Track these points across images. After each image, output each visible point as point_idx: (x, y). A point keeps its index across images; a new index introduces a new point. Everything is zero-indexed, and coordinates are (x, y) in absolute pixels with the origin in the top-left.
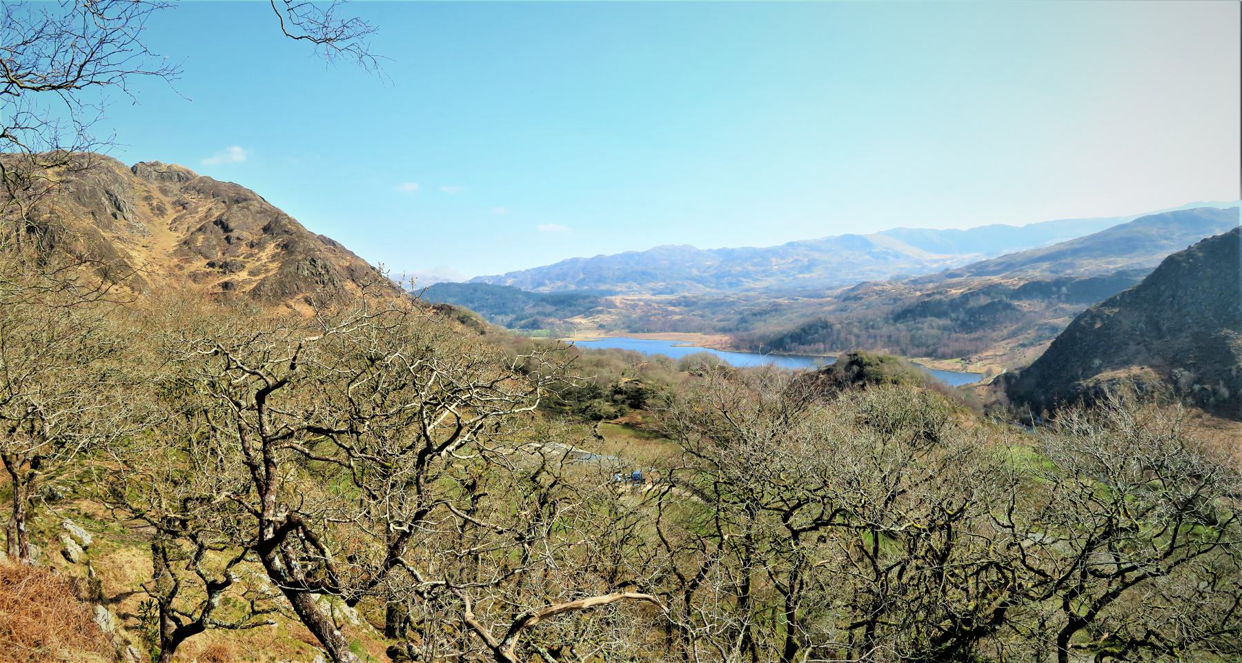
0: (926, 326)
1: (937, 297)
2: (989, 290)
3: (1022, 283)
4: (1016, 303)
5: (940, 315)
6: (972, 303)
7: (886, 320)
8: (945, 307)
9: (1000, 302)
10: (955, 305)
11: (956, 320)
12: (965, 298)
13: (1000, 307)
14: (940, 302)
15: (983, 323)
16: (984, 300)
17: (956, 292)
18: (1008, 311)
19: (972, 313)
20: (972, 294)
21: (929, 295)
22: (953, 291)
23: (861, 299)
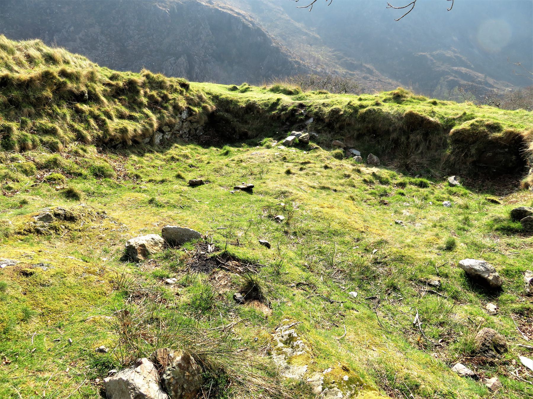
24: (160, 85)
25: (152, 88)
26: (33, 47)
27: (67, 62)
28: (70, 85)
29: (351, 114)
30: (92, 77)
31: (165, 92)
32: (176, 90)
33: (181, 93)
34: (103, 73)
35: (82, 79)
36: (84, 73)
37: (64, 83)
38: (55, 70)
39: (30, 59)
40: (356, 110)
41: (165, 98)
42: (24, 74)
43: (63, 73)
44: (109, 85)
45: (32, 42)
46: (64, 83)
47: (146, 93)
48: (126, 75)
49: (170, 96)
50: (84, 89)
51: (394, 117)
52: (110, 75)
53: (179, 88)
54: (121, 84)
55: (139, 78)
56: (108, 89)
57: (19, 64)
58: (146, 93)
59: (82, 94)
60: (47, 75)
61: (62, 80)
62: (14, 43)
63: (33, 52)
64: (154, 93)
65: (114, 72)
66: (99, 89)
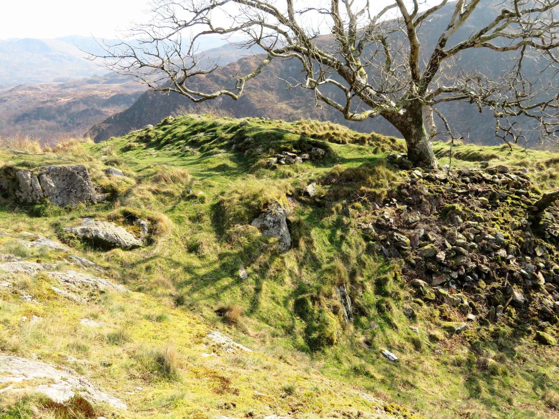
0: (37, 126)
1: (49, 104)
2: (86, 100)
3: (114, 94)
4: (104, 109)
5: (48, 118)
6: (74, 109)
7: (9, 122)
8: (53, 112)
9: (92, 109)
10: (61, 111)
11: (60, 122)
12: (69, 104)
13: (92, 113)
14: (50, 108)
15: (79, 124)
16: (82, 107)
17: (63, 101)
18: (97, 116)
19: (72, 117)
20: (74, 103)
21: (44, 102)
22: (63, 100)
23: (5, 101)
24: (378, 139)
25: (373, 141)
26: (327, 124)
27: (338, 129)
28: (335, 138)
29: (466, 155)
30: (345, 135)
31: (379, 142)
32: (386, 142)
33: (389, 143)
34: (352, 133)
35: (342, 136)
36: (342, 133)
37: (333, 137)
38: (331, 132)
39: (325, 128)
40: (469, 153)
41: (379, 145)
42: (321, 133)
43: (334, 133)
44: (352, 138)
45: (327, 122)
46: (333, 137)
47: (369, 143)
48: (361, 135)
49: (381, 145)
50: (340, 139)
51: (484, 156)
52: (354, 134)
53: (390, 141)
54: (358, 138)
55: (367, 136)
56: (351, 140)
57: (321, 130)
58: (369, 143)
59: (340, 141)
60: (328, 134)
61: (333, 135)
62: (321, 123)
63: (327, 126)
64: (373, 143)
65: (359, 133)
66: (347, 139)
